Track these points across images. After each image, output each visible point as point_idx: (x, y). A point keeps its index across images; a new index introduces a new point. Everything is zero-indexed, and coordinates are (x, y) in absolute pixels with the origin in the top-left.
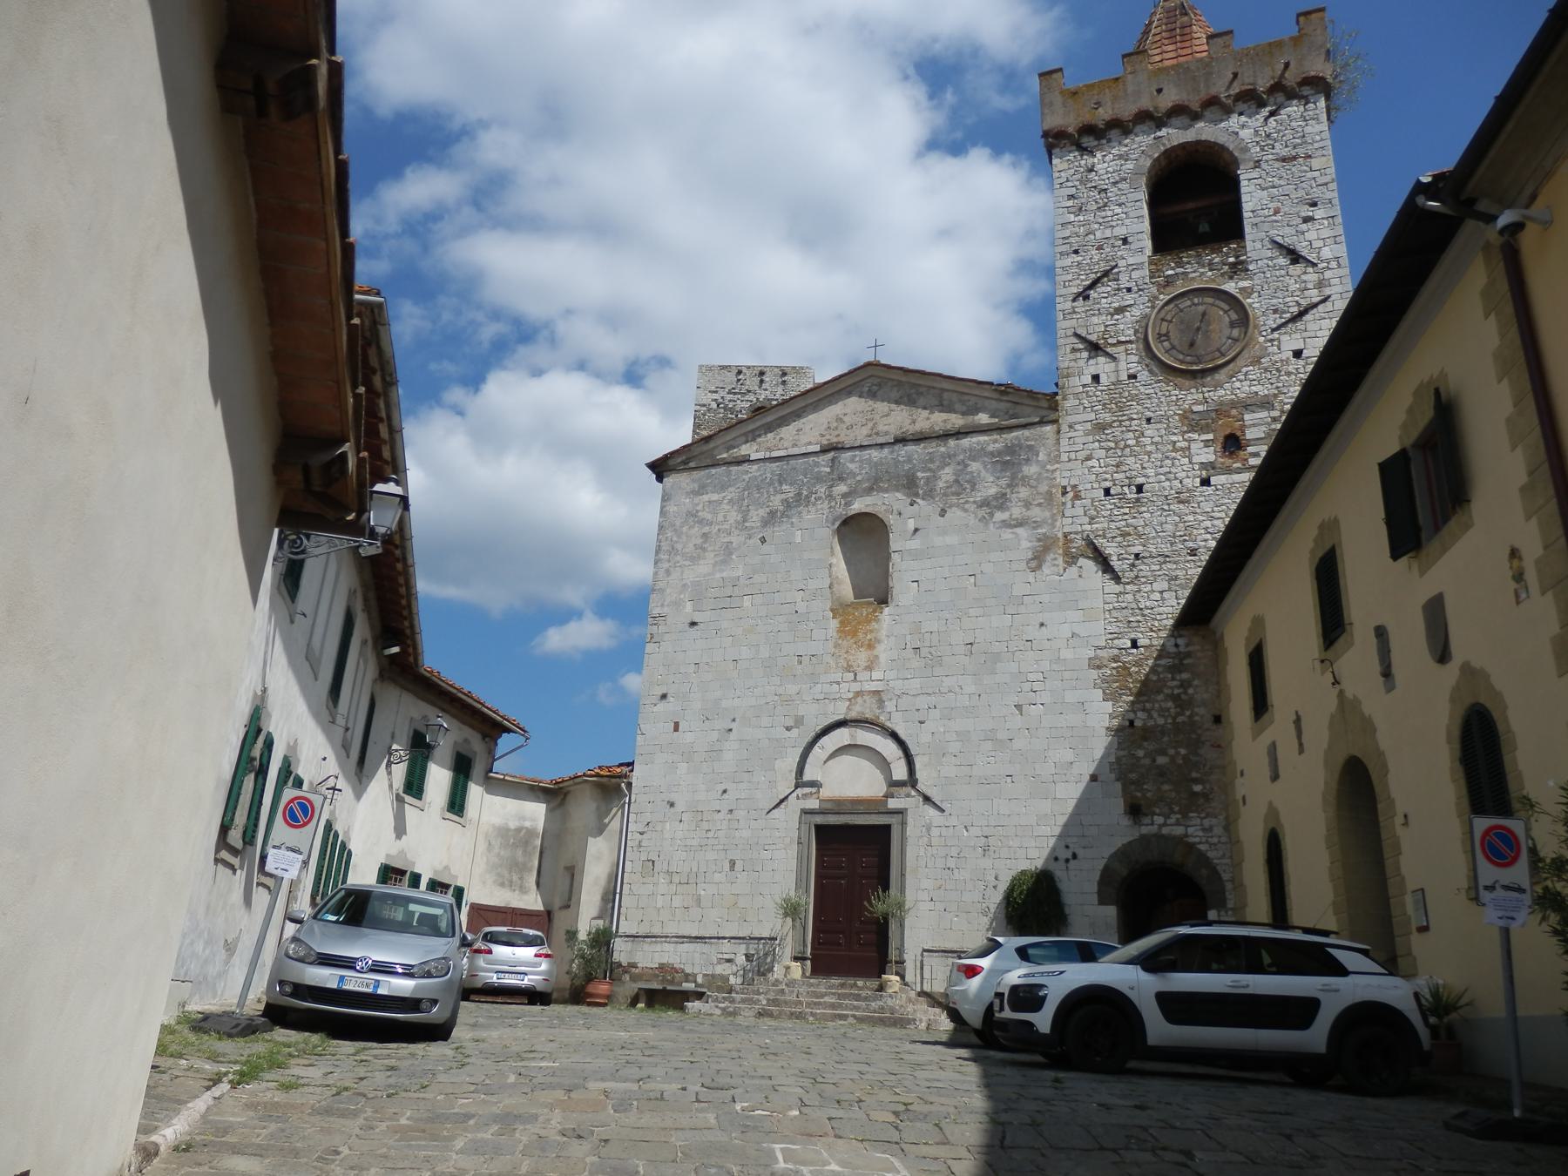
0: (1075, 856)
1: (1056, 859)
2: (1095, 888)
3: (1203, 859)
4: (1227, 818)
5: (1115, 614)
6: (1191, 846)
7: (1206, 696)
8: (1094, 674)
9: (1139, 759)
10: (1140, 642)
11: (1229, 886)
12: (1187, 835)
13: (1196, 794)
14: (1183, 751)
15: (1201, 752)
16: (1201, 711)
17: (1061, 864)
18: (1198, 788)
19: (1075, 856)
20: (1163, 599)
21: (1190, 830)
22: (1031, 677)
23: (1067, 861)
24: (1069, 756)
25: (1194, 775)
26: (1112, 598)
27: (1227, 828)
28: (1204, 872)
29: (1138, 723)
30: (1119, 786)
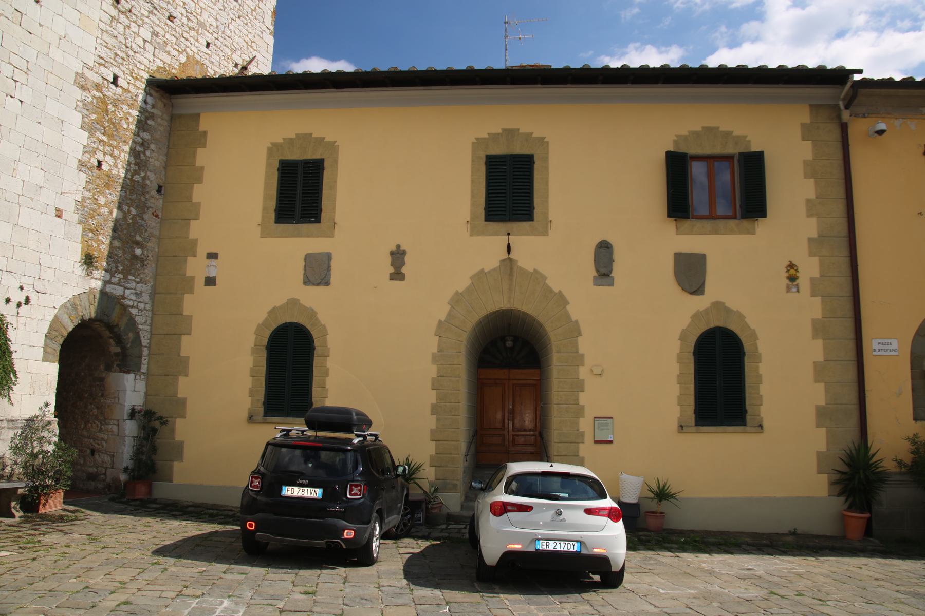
0: (27, 300)
1: (8, 301)
2: (41, 341)
3: (132, 322)
4: (154, 288)
5: (106, 37)
6: (125, 308)
7: (157, 164)
8: (78, 94)
9: (99, 205)
10: (121, 82)
11: (145, 351)
12: (124, 297)
13: (135, 257)
14: (134, 212)
15: (146, 217)
16: (151, 176)
17: (13, 305)
18: (138, 252)
19: (27, 300)
20: (144, 49)
21: (128, 292)
22: (15, 60)
23: (19, 305)
24: (38, 178)
25: (138, 238)
26: (107, 18)
27: (153, 294)
28: (131, 335)
29: (105, 167)
30: (80, 229)
